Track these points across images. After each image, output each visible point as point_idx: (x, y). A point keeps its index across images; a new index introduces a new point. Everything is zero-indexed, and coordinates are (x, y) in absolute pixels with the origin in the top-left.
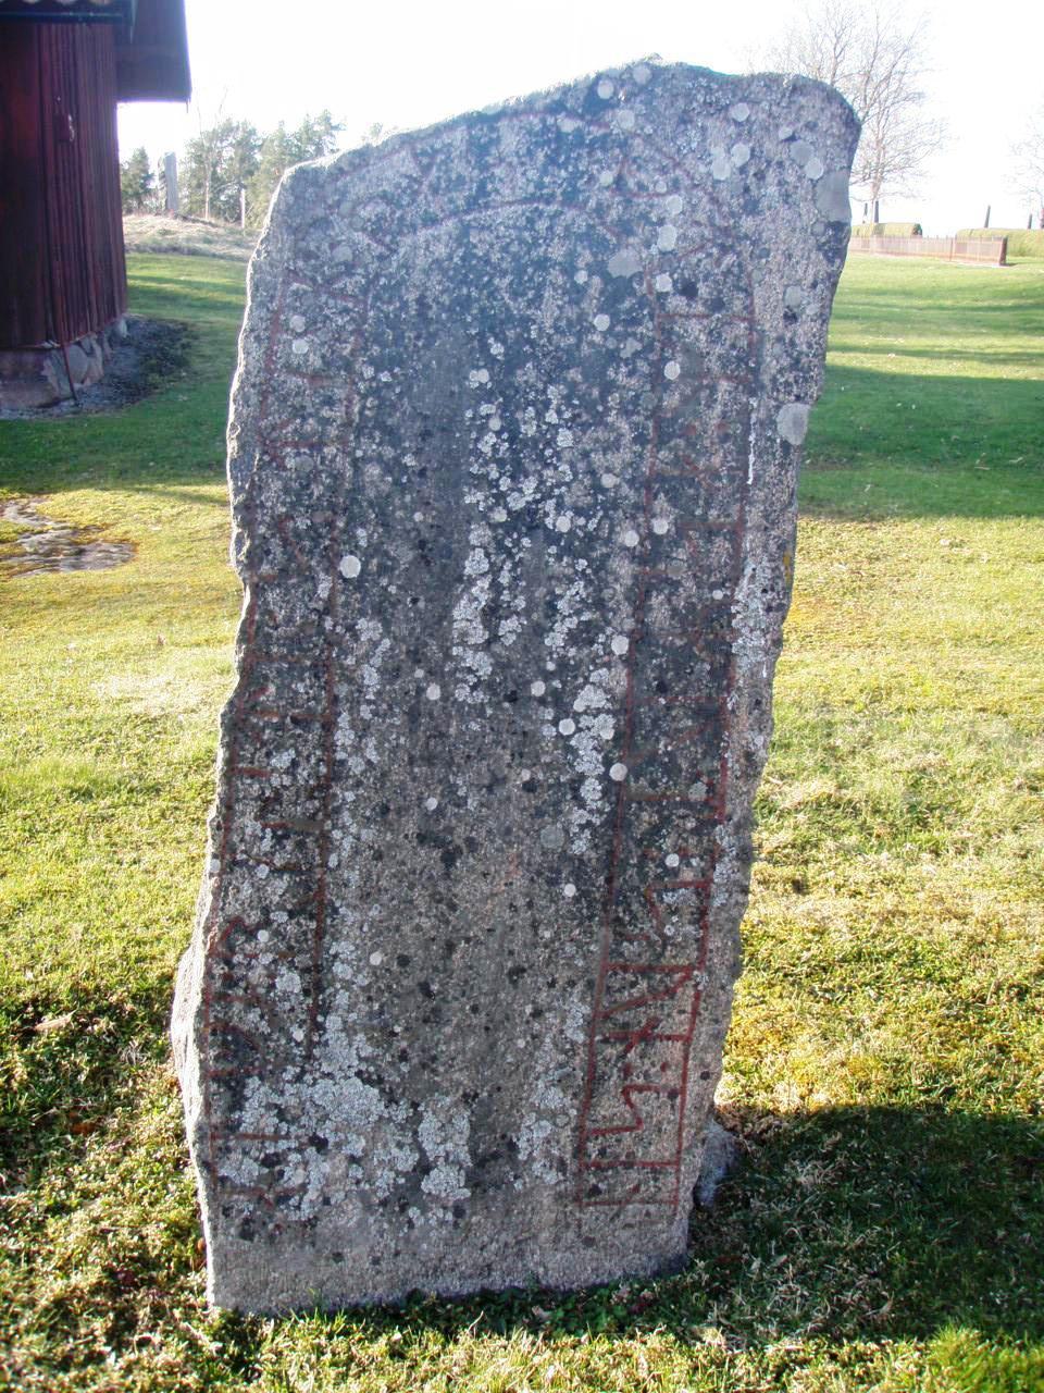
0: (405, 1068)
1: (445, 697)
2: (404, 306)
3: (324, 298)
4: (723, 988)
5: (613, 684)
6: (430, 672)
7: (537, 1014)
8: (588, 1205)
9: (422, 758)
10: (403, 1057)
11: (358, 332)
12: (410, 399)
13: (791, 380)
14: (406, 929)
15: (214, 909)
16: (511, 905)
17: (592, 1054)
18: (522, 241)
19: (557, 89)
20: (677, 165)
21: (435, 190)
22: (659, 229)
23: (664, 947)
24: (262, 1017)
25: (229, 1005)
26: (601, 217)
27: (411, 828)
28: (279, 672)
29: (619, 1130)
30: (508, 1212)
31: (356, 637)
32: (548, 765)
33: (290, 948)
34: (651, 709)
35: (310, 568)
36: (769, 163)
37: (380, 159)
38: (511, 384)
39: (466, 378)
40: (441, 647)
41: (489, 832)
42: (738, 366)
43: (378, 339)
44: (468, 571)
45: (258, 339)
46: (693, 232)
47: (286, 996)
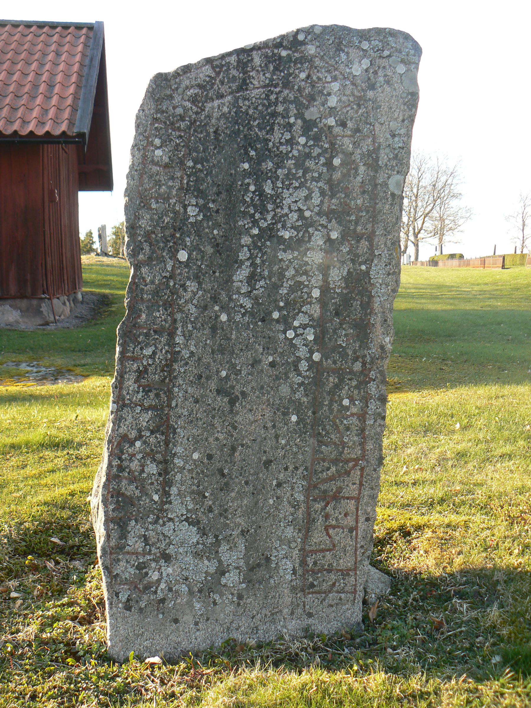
0: (211, 515)
1: (229, 320)
2: (208, 134)
3: (170, 131)
4: (375, 470)
5: (313, 312)
6: (222, 308)
7: (279, 485)
8: (309, 593)
9: (218, 350)
10: (210, 510)
11: (187, 146)
12: (211, 177)
13: (394, 165)
14: (211, 440)
15: (113, 430)
16: (264, 426)
17: (308, 508)
18: (264, 105)
19: (278, 37)
20: (336, 69)
21: (222, 83)
22: (329, 98)
23: (343, 448)
24: (137, 488)
25: (121, 481)
26: (300, 93)
27: (213, 385)
28: (147, 307)
29: (323, 551)
30: (266, 597)
31: (185, 290)
32: (281, 353)
33: (152, 450)
34: (332, 325)
35: (163, 257)
36: (379, 68)
37: (197, 69)
38: (260, 169)
39: (238, 167)
40: (227, 295)
41: (252, 388)
42: (368, 159)
43: (196, 150)
44: (240, 258)
45: (139, 149)
46: (344, 98)
47: (150, 475)
